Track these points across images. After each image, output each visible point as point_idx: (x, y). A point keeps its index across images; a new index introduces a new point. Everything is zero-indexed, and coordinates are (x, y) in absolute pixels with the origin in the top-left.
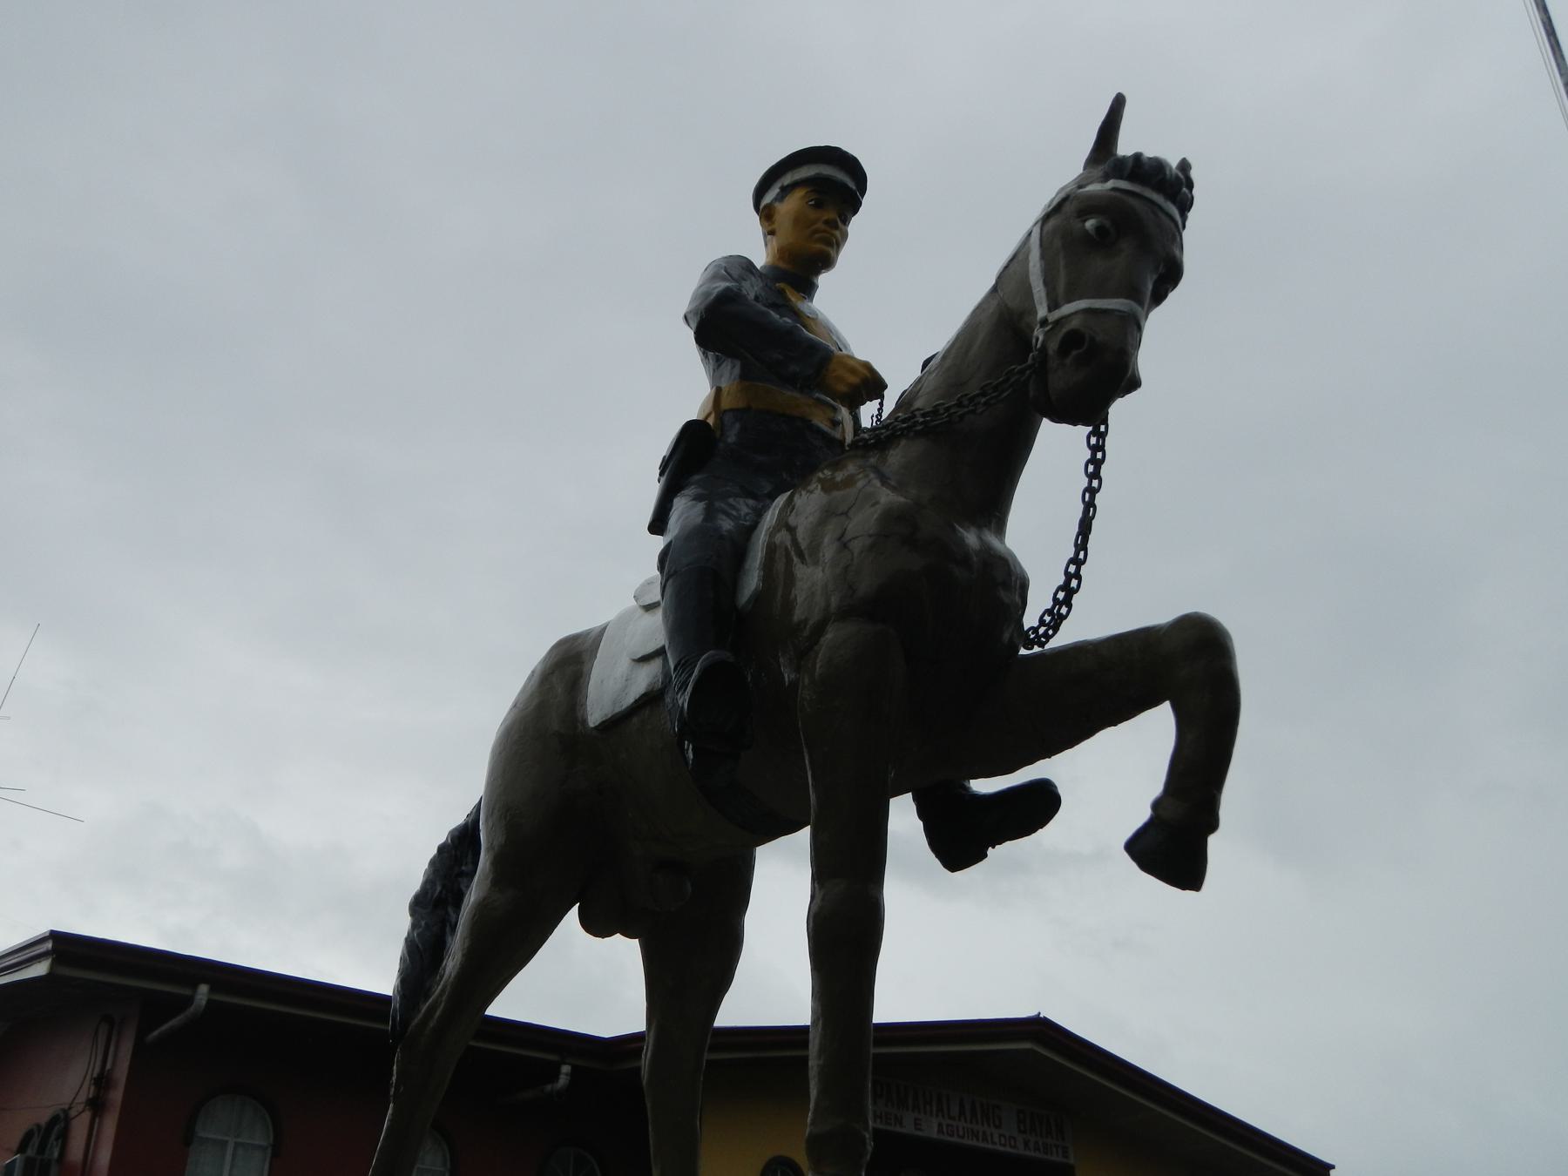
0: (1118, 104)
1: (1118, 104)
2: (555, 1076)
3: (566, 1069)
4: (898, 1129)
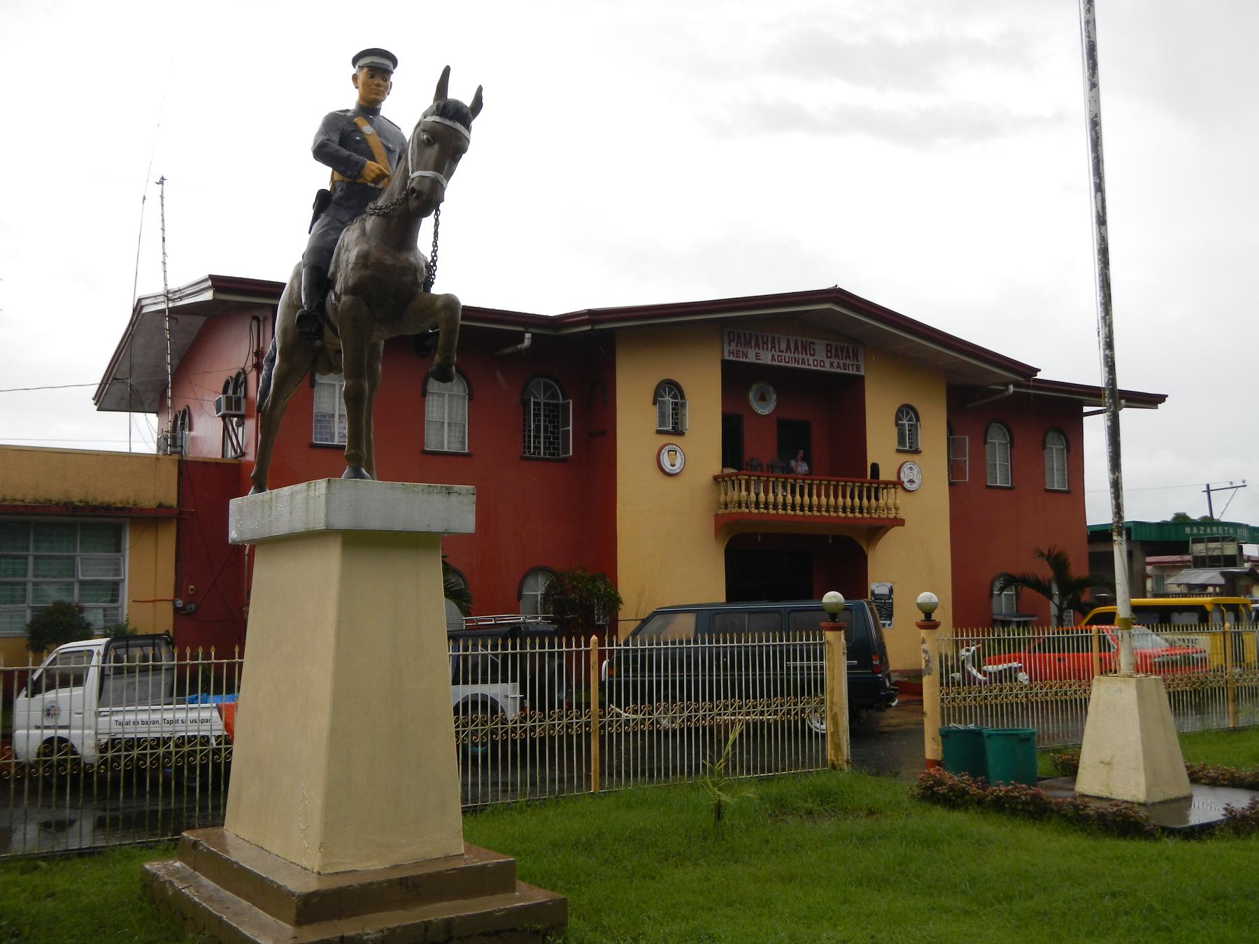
0: (447, 72)
1: (447, 72)
2: (522, 341)
3: (528, 336)
4: (745, 360)
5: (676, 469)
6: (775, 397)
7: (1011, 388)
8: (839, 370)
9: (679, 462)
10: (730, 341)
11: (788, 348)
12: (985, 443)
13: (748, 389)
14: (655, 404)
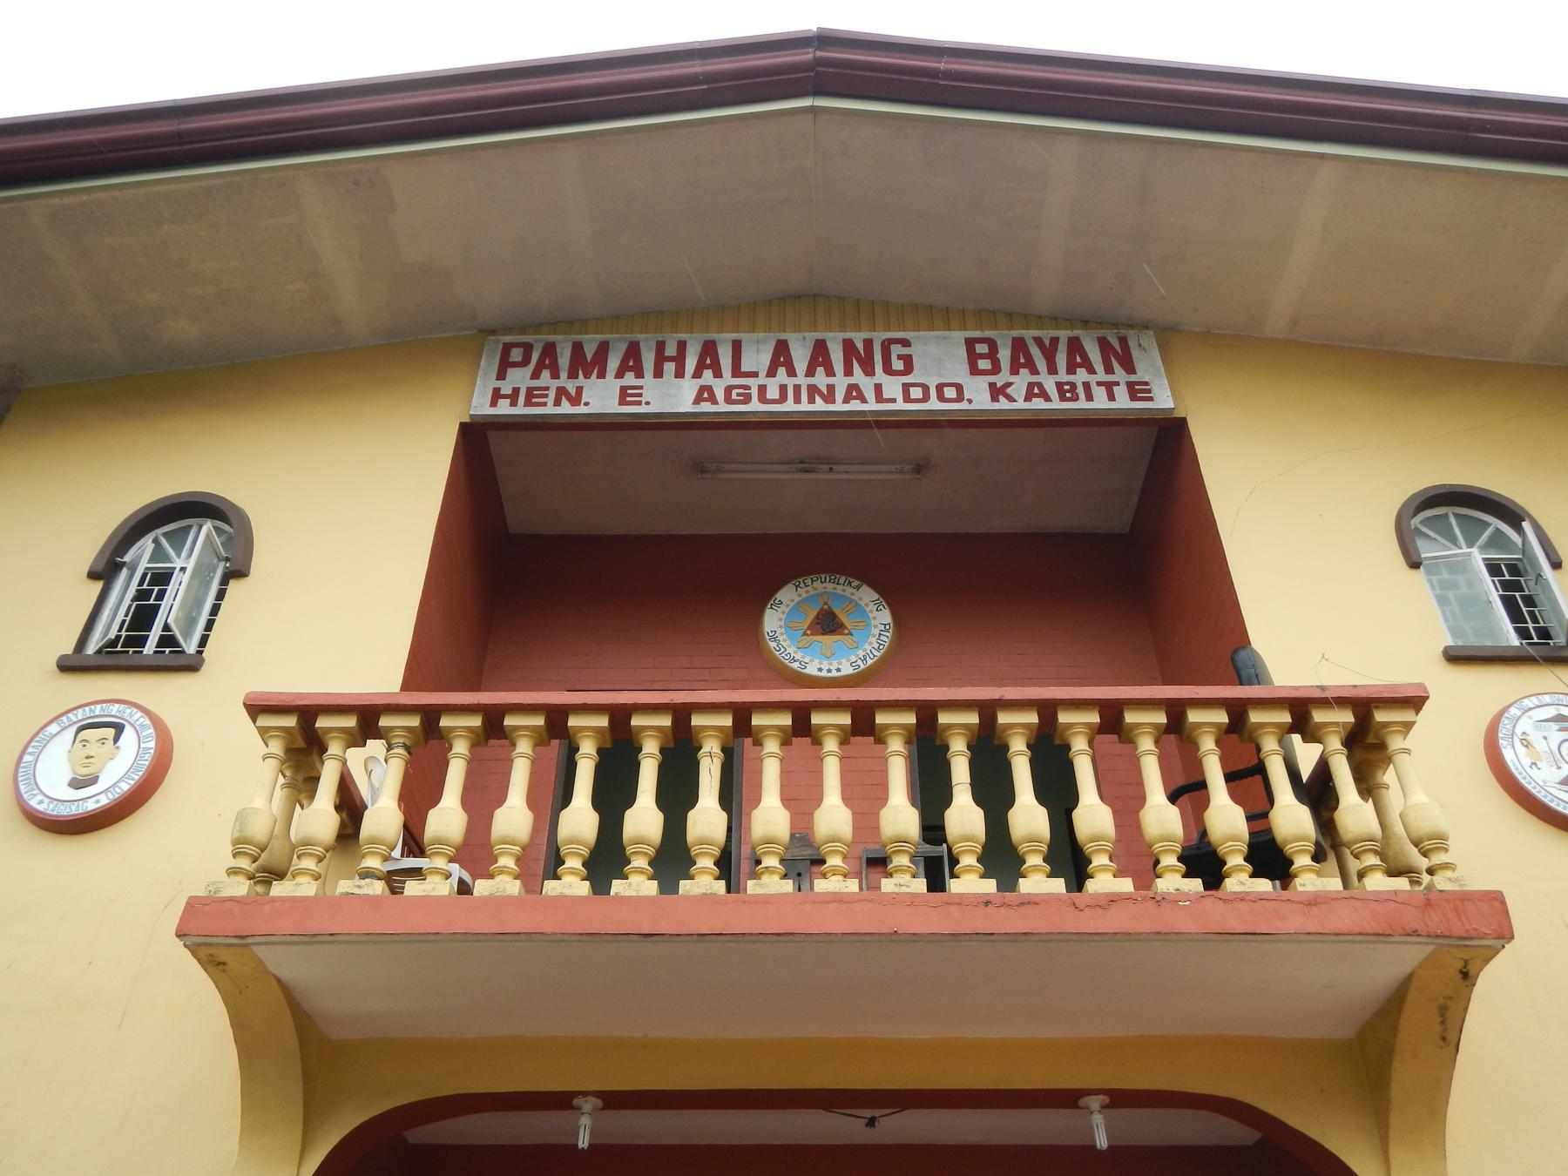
4: (566, 408)
6: (885, 616)
8: (1038, 404)
9: (119, 769)
11: (781, 358)
13: (763, 596)
14: (105, 571)
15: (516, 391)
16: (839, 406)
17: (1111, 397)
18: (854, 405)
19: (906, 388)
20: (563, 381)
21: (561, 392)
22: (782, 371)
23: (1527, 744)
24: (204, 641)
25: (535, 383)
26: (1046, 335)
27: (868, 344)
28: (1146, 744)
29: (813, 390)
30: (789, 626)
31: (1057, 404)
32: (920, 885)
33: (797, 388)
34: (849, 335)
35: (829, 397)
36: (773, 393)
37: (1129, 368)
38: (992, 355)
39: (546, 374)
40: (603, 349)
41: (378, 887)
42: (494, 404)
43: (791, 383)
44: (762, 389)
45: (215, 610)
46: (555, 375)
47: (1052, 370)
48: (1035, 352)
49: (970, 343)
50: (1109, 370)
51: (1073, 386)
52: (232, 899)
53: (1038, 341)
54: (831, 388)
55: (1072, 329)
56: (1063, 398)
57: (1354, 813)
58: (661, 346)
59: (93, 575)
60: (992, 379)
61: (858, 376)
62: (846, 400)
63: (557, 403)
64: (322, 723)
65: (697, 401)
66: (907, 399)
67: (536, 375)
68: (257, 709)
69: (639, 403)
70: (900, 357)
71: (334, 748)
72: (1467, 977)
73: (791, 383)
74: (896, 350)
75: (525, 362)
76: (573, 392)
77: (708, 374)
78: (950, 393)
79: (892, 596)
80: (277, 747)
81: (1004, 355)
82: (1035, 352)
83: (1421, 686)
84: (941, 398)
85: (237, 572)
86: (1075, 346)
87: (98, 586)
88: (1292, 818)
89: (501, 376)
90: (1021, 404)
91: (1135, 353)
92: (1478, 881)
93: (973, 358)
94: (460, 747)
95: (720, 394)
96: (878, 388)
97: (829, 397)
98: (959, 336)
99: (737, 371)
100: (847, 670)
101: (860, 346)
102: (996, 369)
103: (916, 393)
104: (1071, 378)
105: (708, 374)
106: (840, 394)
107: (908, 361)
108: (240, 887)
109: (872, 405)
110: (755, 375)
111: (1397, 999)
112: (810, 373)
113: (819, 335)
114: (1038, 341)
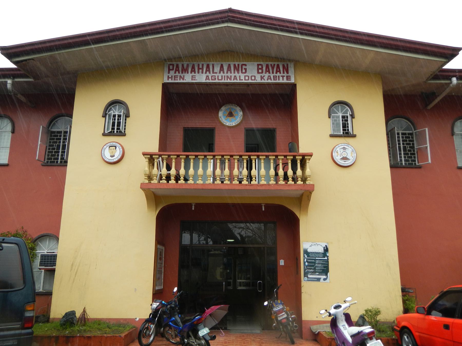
4: (182, 81)
5: (115, 159)
6: (241, 113)
7: (454, 80)
8: (269, 81)
9: (118, 154)
10: (169, 70)
12: (453, 134)
14: (104, 116)
15: (172, 76)
16: (232, 81)
17: (283, 80)
18: (235, 81)
19: (245, 76)
20: (181, 74)
21: (180, 76)
22: (222, 72)
23: (337, 152)
24: (125, 129)
25: (175, 75)
26: (273, 63)
27: (238, 65)
28: (272, 161)
29: (228, 77)
30: (224, 115)
31: (273, 81)
32: (238, 182)
33: (225, 76)
34: (235, 63)
35: (231, 79)
36: (220, 78)
37: (288, 73)
38: (262, 69)
39: (177, 72)
40: (188, 65)
41: (166, 182)
42: (168, 80)
43: (223, 75)
44: (218, 76)
45: (125, 123)
46: (179, 73)
47: (273, 73)
48: (270, 68)
49: (258, 65)
50: (284, 73)
51: (276, 76)
52: (146, 183)
53: (271, 65)
54: (231, 76)
55: (278, 62)
56: (274, 80)
57: (299, 172)
58: (199, 65)
59: (103, 117)
60: (261, 75)
61: (236, 74)
62: (234, 80)
63: (180, 80)
64: (154, 157)
65: (206, 80)
66: (245, 80)
67: (175, 73)
68: (144, 154)
69: (195, 80)
70: (244, 69)
71: (156, 160)
72: (311, 193)
73: (223, 75)
74: (244, 67)
75: (173, 69)
76: (182, 77)
77: (208, 72)
78: (253, 78)
79: (243, 109)
80: (147, 160)
81: (264, 68)
82: (270, 68)
83: (312, 153)
84: (251, 80)
85: (127, 116)
86: (278, 66)
87: (104, 118)
88: (290, 172)
89: (169, 73)
90: (266, 81)
91: (289, 69)
92: (311, 183)
93: (258, 69)
94: (174, 160)
95: (210, 78)
96: (240, 76)
97: (231, 79)
98: (256, 63)
99: (213, 73)
100: (234, 124)
101: (237, 66)
102: (262, 73)
103: (247, 78)
104: (276, 75)
105: (208, 72)
106: (232, 79)
107: (246, 69)
108: (147, 182)
109: (238, 81)
110: (216, 73)
111: (302, 195)
112: (227, 73)
113: (229, 63)
114: (271, 65)
